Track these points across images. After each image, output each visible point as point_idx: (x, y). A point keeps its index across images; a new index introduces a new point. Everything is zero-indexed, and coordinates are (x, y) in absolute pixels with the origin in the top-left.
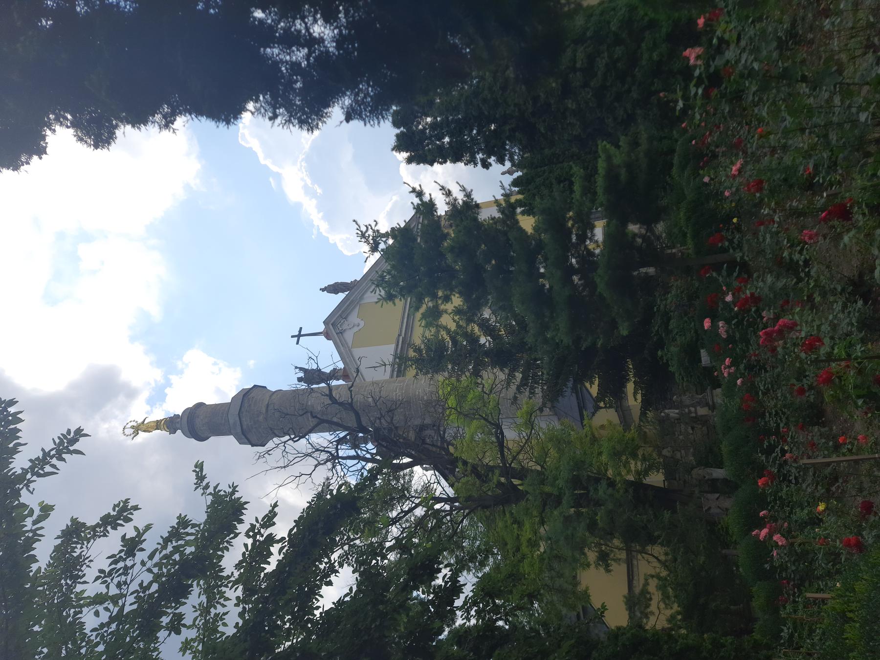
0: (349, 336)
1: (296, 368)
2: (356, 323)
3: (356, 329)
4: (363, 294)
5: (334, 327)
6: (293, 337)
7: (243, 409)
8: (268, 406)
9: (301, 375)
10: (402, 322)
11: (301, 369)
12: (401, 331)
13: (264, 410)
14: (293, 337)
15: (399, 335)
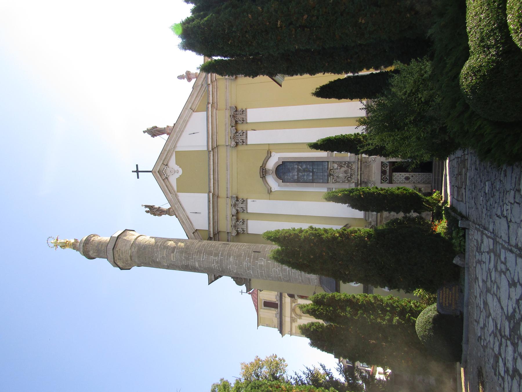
0: (173, 180)
1: (142, 206)
2: (176, 170)
3: (177, 176)
4: (176, 144)
5: (160, 173)
6: (133, 172)
7: (115, 259)
8: (131, 257)
9: (148, 209)
10: (210, 179)
11: (146, 206)
12: (210, 187)
13: (129, 258)
14: (133, 172)
15: (210, 192)
